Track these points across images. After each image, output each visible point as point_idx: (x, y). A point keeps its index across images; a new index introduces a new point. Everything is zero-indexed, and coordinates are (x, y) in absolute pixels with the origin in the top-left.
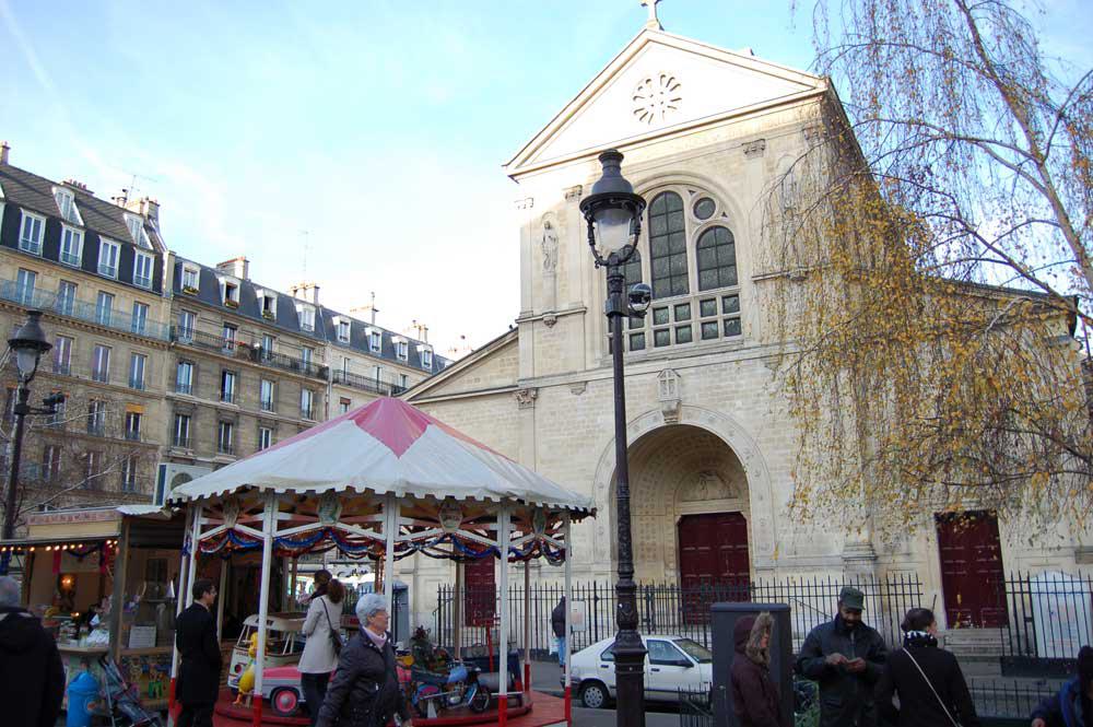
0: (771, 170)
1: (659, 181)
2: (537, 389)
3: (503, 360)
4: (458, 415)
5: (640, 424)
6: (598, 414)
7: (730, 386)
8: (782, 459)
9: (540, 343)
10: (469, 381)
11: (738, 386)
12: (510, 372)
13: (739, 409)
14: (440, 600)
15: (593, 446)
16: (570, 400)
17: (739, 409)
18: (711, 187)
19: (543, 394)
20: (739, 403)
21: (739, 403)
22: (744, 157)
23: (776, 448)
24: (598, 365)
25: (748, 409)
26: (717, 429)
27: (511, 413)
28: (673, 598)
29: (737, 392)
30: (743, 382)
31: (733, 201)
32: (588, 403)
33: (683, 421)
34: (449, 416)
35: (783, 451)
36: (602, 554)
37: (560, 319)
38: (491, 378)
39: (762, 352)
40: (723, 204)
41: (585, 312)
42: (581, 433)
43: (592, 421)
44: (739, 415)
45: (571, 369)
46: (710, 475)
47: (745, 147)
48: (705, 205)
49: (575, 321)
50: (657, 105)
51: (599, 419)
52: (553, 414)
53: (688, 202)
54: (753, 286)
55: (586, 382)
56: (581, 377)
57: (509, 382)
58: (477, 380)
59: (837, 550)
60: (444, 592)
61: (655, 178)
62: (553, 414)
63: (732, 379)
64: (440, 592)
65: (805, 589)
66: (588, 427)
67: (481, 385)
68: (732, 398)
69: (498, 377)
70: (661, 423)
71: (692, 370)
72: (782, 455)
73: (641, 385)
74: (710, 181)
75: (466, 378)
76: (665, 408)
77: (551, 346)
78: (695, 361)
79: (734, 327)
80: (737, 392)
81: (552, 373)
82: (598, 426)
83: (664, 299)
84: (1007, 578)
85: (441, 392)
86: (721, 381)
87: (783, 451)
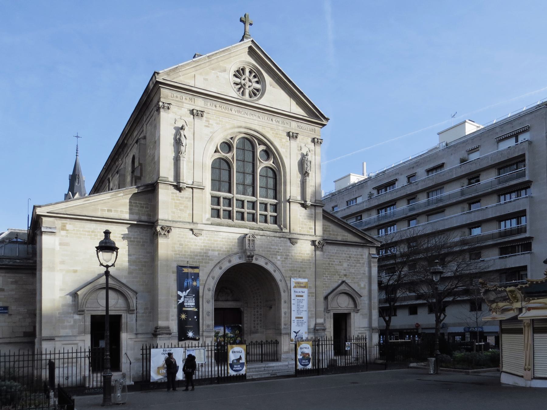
5: (232, 259)
7: (276, 249)
9: (174, 199)
11: (280, 249)
15: (206, 267)
17: (279, 260)
20: (279, 258)
21: (279, 258)
24: (210, 223)
27: (137, 238)
29: (278, 252)
30: (281, 248)
33: (254, 261)
38: (123, 211)
42: (199, 259)
44: (279, 263)
56: (200, 227)
63: (277, 246)
66: (203, 256)
68: (276, 255)
76: (249, 254)
77: (181, 204)
80: (278, 252)
81: (181, 220)
82: (209, 257)
84: (44, 352)
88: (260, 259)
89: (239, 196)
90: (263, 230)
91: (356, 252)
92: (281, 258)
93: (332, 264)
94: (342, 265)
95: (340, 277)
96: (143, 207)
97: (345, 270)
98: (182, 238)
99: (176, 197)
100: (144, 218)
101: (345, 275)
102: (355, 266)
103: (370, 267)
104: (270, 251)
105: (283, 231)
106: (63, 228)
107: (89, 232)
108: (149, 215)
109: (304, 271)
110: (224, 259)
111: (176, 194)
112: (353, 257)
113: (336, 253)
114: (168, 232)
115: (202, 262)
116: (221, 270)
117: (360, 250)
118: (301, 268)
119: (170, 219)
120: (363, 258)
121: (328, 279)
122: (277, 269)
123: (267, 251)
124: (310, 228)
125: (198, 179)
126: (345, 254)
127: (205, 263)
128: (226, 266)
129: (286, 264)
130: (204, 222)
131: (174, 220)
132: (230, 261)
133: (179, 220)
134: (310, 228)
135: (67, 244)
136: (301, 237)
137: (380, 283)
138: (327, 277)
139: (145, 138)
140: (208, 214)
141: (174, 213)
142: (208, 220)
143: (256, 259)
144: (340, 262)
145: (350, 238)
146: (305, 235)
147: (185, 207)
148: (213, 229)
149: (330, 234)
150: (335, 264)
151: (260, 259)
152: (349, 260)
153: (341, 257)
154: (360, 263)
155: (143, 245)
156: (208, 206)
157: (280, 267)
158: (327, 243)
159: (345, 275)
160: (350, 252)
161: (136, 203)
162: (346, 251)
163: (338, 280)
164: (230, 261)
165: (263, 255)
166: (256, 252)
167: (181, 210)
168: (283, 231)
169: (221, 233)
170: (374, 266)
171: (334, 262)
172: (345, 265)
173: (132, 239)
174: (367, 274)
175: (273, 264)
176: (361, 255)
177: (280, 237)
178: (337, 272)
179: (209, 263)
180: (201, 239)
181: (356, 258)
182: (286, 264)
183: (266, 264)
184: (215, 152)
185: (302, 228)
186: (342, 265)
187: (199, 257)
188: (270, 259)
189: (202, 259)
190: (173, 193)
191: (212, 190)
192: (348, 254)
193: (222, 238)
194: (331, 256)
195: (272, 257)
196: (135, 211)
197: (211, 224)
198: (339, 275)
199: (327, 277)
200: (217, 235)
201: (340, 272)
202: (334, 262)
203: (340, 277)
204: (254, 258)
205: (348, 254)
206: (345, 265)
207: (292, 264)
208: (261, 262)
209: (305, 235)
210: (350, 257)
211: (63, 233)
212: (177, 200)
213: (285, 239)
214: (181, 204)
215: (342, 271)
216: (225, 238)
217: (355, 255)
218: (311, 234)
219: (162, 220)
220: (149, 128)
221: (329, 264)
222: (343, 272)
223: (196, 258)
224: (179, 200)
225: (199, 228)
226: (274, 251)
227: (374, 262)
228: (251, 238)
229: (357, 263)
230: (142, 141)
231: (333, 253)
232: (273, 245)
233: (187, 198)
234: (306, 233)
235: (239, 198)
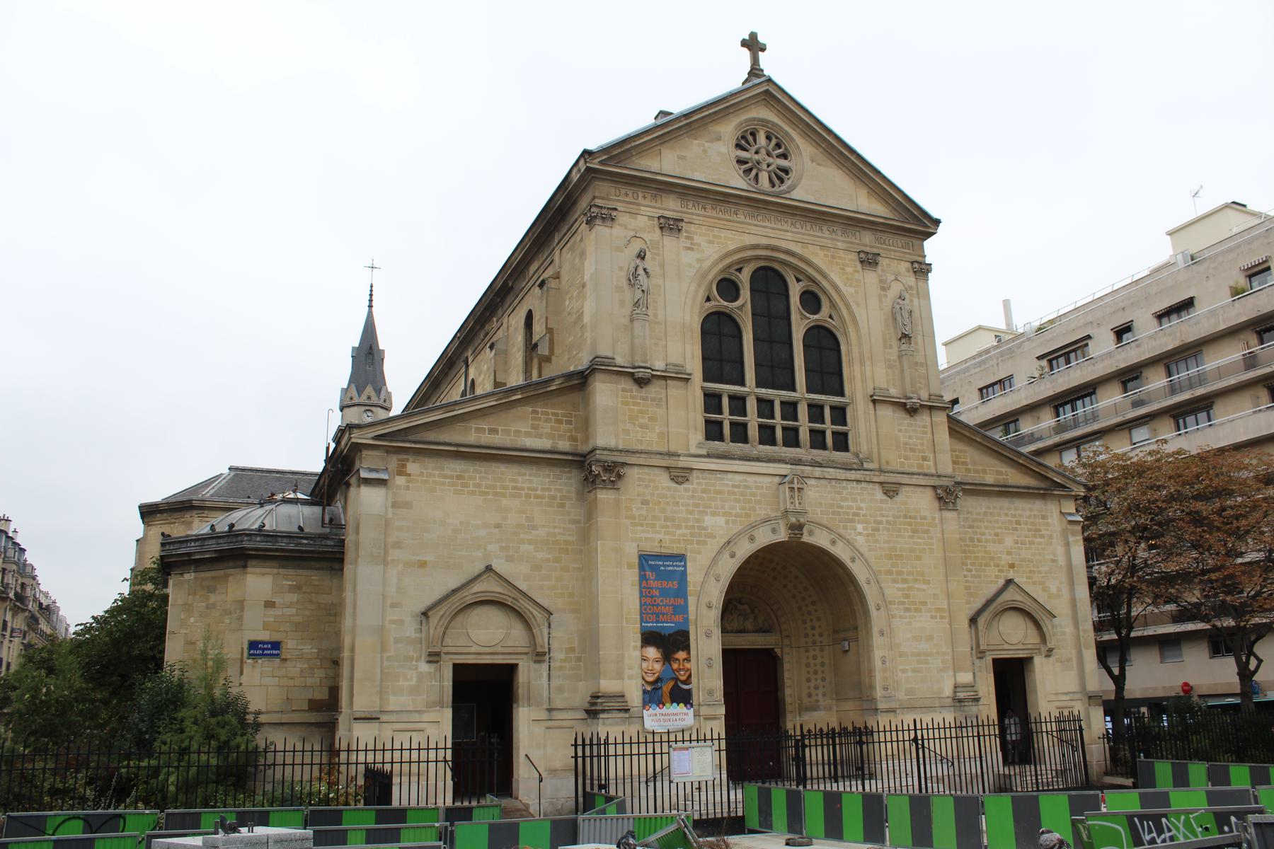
0: (883, 289)
1: (769, 253)
2: (624, 464)
3: (534, 412)
4: (459, 477)
5: (756, 533)
6: (706, 513)
7: (851, 507)
8: (900, 593)
10: (479, 430)
11: (860, 509)
12: (549, 431)
13: (860, 534)
14: (576, 757)
15: (699, 553)
16: (669, 489)
17: (860, 534)
18: (825, 283)
19: (633, 474)
20: (860, 527)
21: (860, 527)
22: (859, 265)
23: (895, 581)
24: (704, 452)
25: (868, 535)
26: (841, 552)
27: (549, 490)
28: (822, 745)
29: (857, 515)
31: (848, 306)
32: (693, 497)
33: (806, 538)
34: (440, 475)
35: (901, 586)
36: (711, 692)
37: (655, 381)
38: (518, 432)
39: (881, 479)
40: (833, 305)
41: (688, 380)
43: (698, 521)
44: (860, 541)
45: (673, 449)
46: (741, 603)
47: (862, 255)
48: (811, 301)
49: (675, 390)
50: (764, 167)
51: (709, 520)
52: (645, 502)
53: (795, 291)
54: (871, 405)
55: (692, 469)
56: (684, 462)
57: (545, 444)
58: (492, 431)
59: (948, 691)
60: (584, 745)
61: (767, 247)
62: (645, 502)
63: (854, 500)
64: (576, 745)
65: (627, 747)
67: (498, 439)
68: (853, 521)
69: (528, 434)
70: (783, 536)
71: (813, 482)
72: (898, 589)
73: (757, 488)
74: (825, 276)
75: (473, 425)
76: (793, 520)
77: (642, 412)
78: (818, 472)
79: (842, 442)
80: (857, 515)
82: (705, 529)
83: (770, 391)
85: (431, 436)
86: (843, 499)
87: (901, 586)
88: (817, 531)
89: (763, 391)
90: (821, 466)
91: (1031, 510)
92: (865, 529)
93: (979, 541)
94: (1001, 542)
95: (1000, 571)
96: (560, 422)
97: (1009, 553)
98: (647, 486)
99: (632, 397)
100: (564, 445)
101: (1012, 566)
102: (1032, 543)
103: (1067, 545)
104: (839, 514)
105: (866, 465)
106: (401, 472)
107: (452, 477)
108: (573, 439)
109: (919, 558)
110: (739, 534)
111: (631, 391)
112: (1026, 523)
113: (985, 514)
114: (619, 476)
115: (692, 543)
116: (733, 560)
117: (1037, 506)
118: (912, 550)
119: (621, 447)
120: (1048, 524)
121: (973, 576)
122: (858, 554)
123: (834, 513)
124: (925, 459)
125: (675, 358)
126: (1006, 515)
127: (698, 543)
128: (745, 549)
129: (877, 541)
130: (693, 450)
131: (628, 448)
132: (752, 539)
133: (639, 447)
134: (925, 459)
135: (407, 505)
136: (905, 479)
137: (1092, 581)
138: (970, 570)
139: (557, 276)
140: (699, 436)
141: (626, 432)
142: (699, 446)
143: (811, 533)
144: (997, 535)
145: (1014, 477)
146: (913, 474)
147: (650, 419)
148: (713, 467)
149: (968, 470)
150: (987, 541)
151: (817, 531)
152: (1016, 529)
153: (997, 522)
154: (1042, 536)
155: (562, 505)
156: (697, 416)
157: (864, 551)
158: (964, 491)
159: (1012, 566)
160: (1016, 509)
161: (547, 414)
162: (1009, 509)
163: (997, 577)
164: (752, 539)
165: (825, 523)
166: (810, 516)
167: (642, 426)
168: (866, 465)
169: (730, 476)
170: (1077, 541)
171: (983, 534)
172: (1009, 541)
173: (539, 492)
174: (1062, 561)
175: (849, 542)
176: (1044, 517)
177: (858, 481)
178: (992, 559)
179: (705, 543)
180: (687, 490)
181: (1032, 524)
182: (877, 541)
183: (833, 542)
184: (708, 299)
185: (907, 458)
186: (1001, 542)
187: (683, 531)
188: (841, 531)
189: (692, 535)
190: (624, 390)
191: (706, 379)
192: (1013, 516)
193: (733, 486)
194: (975, 520)
195: (845, 528)
196: (545, 431)
197: (708, 456)
198: (997, 565)
199: (970, 570)
200: (722, 479)
201: (1000, 558)
202: (983, 534)
203: (1000, 571)
204: (805, 530)
205: (1013, 516)
206: (1009, 541)
207: (888, 542)
208: (820, 539)
209: (913, 474)
210: (1018, 523)
211: (400, 480)
212: (636, 404)
213: (871, 486)
214: (642, 412)
215: (1004, 556)
216: (738, 487)
217: (1030, 517)
218: (926, 471)
219: (604, 449)
220: (567, 255)
221: (972, 540)
222: (1005, 559)
223: (679, 532)
224: (638, 404)
225: (681, 464)
226: (848, 514)
227: (1074, 533)
228: (796, 486)
229: (1035, 536)
230: (553, 284)
231: (978, 514)
232: (847, 500)
233: (653, 400)
234: (916, 470)
235: (765, 397)
